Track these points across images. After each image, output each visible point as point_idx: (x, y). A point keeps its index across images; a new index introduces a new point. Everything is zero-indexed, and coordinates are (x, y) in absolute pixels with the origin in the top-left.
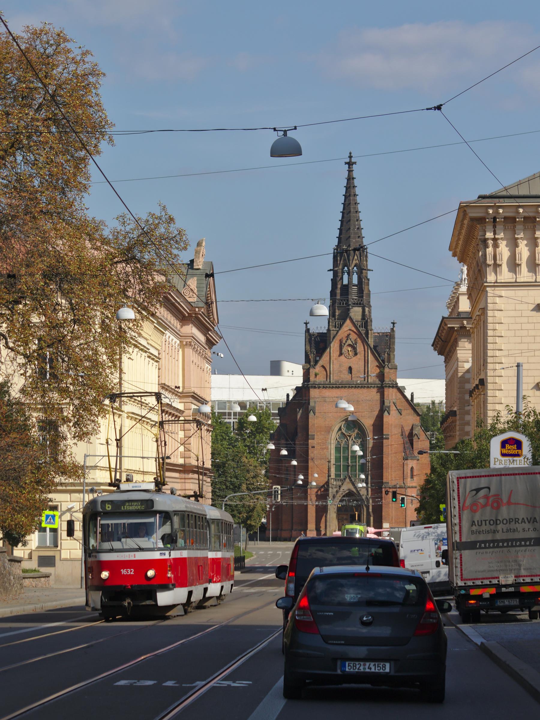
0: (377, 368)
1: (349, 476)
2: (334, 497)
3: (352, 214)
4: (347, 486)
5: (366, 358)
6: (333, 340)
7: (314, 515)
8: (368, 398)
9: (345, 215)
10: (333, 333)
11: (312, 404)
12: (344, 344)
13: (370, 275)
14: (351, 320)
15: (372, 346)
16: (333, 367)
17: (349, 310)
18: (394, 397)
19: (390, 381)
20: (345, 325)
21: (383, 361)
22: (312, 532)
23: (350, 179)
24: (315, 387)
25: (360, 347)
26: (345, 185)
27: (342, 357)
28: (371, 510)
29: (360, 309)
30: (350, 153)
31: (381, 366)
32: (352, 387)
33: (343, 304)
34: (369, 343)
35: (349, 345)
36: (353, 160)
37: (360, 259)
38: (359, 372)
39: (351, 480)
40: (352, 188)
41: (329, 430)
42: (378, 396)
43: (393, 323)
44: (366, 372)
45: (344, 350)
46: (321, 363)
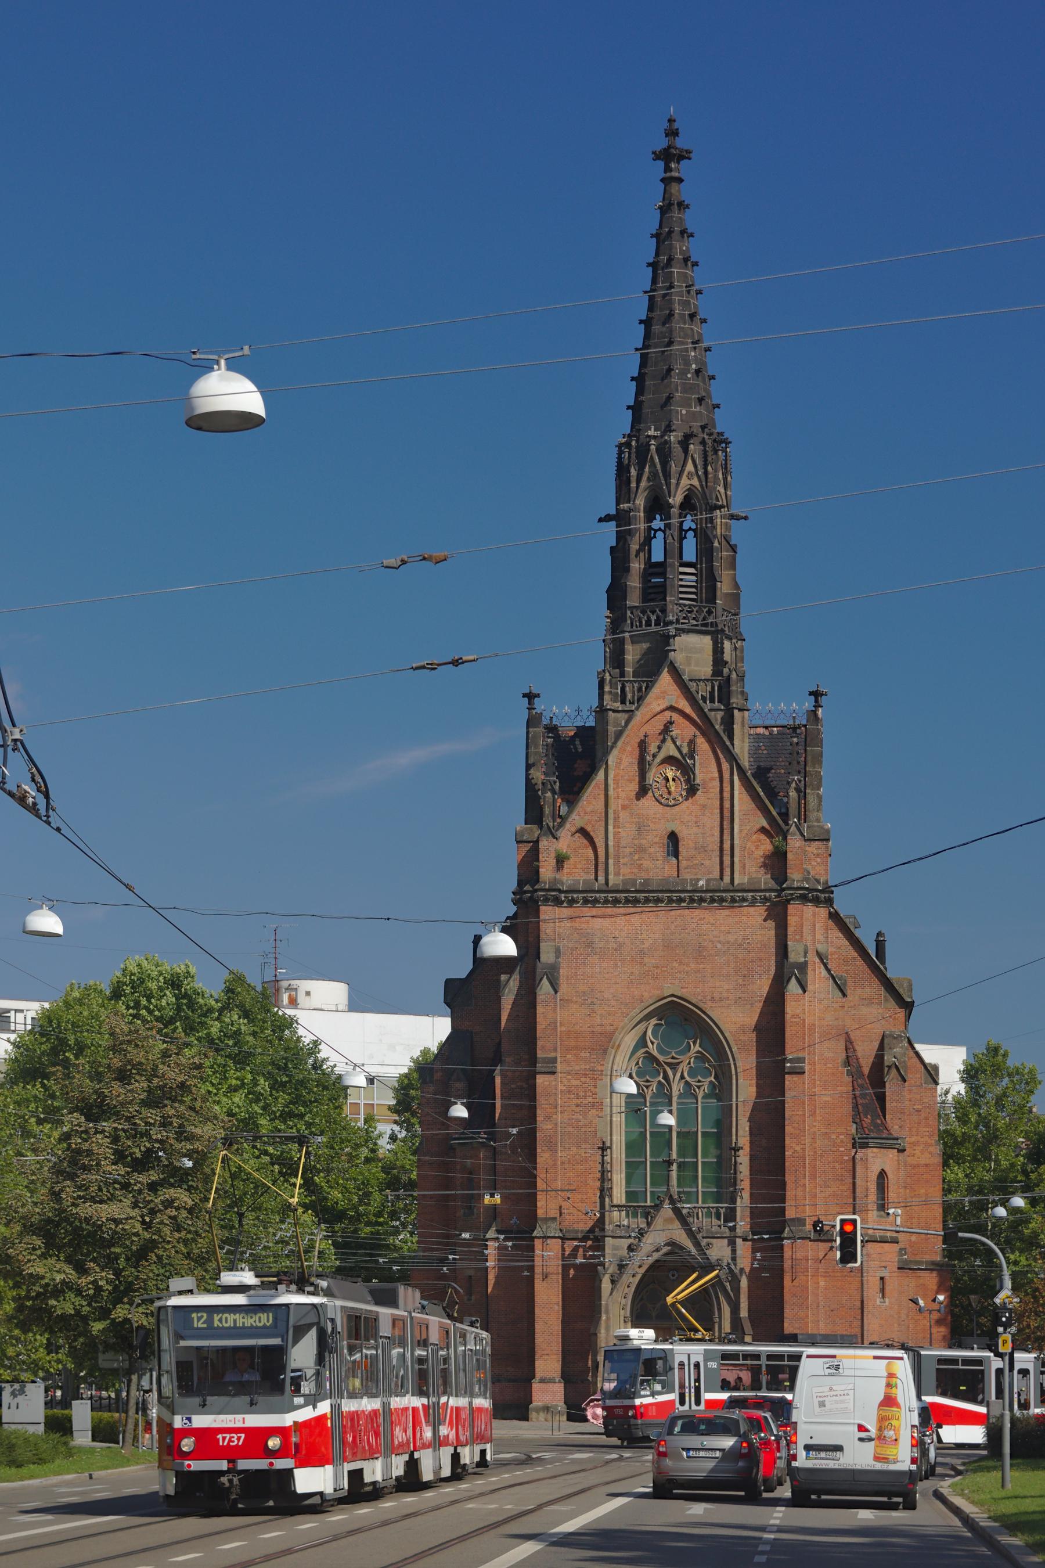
0: (763, 837)
1: (671, 1196)
2: (621, 1267)
3: (676, 324)
4: (665, 1231)
5: (727, 804)
6: (615, 742)
7: (556, 1326)
8: (731, 938)
9: (656, 328)
12: (654, 756)
14: (676, 674)
15: (745, 763)
16: (616, 834)
17: (666, 639)
18: (819, 936)
19: (807, 880)
20: (655, 691)
21: (785, 816)
22: (551, 1385)
24: (558, 902)
25: (705, 768)
26: (654, 227)
27: (648, 801)
28: (744, 1313)
29: (707, 641)
30: (671, 121)
31: (776, 829)
32: (681, 900)
33: (648, 624)
34: (737, 750)
35: (670, 760)
36: (680, 143)
37: (706, 473)
39: (677, 1212)
40: (676, 236)
41: (603, 1044)
42: (769, 932)
44: (726, 852)
45: (653, 776)
46: (576, 820)
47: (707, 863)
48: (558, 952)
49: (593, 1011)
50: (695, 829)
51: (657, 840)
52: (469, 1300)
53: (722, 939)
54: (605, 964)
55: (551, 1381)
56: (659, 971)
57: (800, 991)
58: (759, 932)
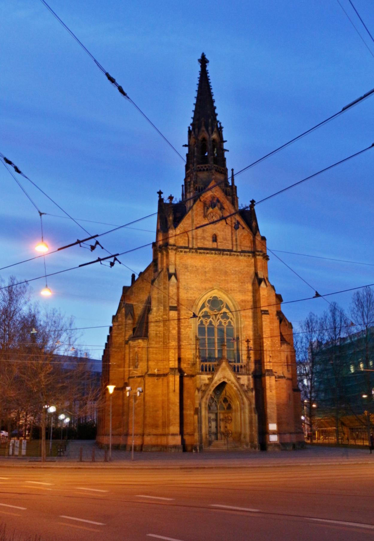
8: (237, 269)
10: (189, 204)
11: (172, 270)
23: (204, 74)
53: (234, 269)
54: (192, 275)
57: (265, 286)
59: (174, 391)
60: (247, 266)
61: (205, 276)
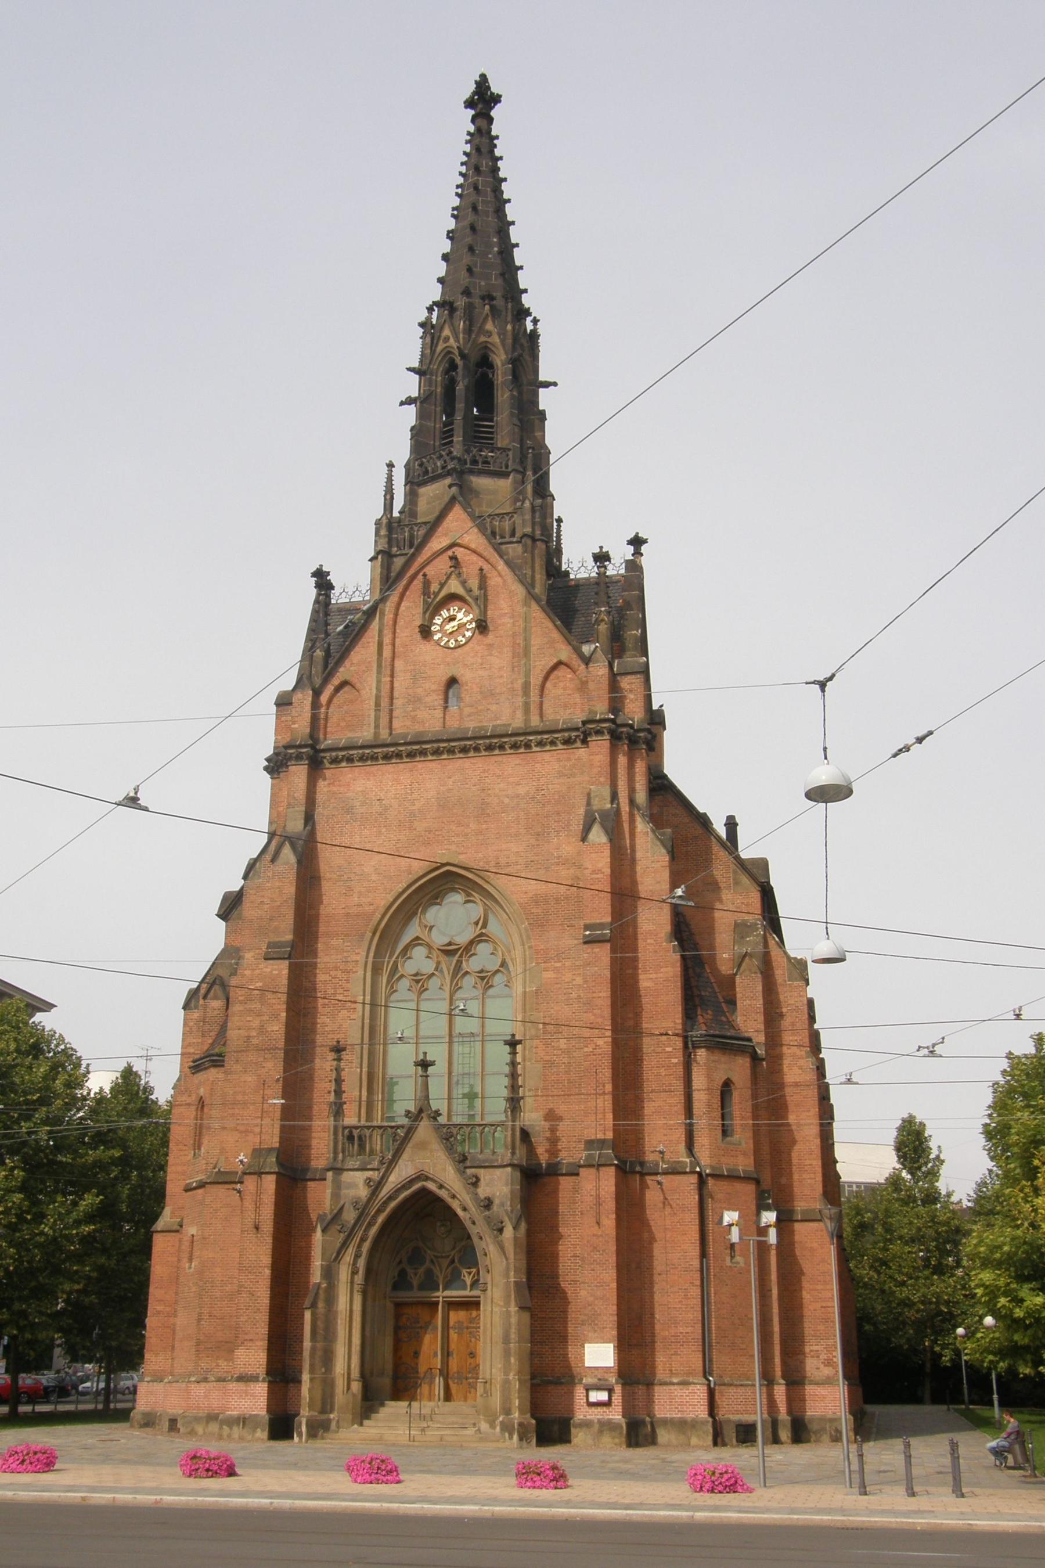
8: (521, 790)
13: (545, 399)
22: (252, 1385)
35: (453, 597)
38: (489, 694)
43: (637, 542)
47: (494, 708)
48: (309, 818)
49: (350, 889)
50: (481, 673)
51: (434, 687)
52: (190, 1268)
53: (509, 792)
54: (366, 832)
55: (254, 1379)
56: (431, 836)
58: (556, 781)
59: (257, 1228)
60: (561, 774)
61: (410, 829)
